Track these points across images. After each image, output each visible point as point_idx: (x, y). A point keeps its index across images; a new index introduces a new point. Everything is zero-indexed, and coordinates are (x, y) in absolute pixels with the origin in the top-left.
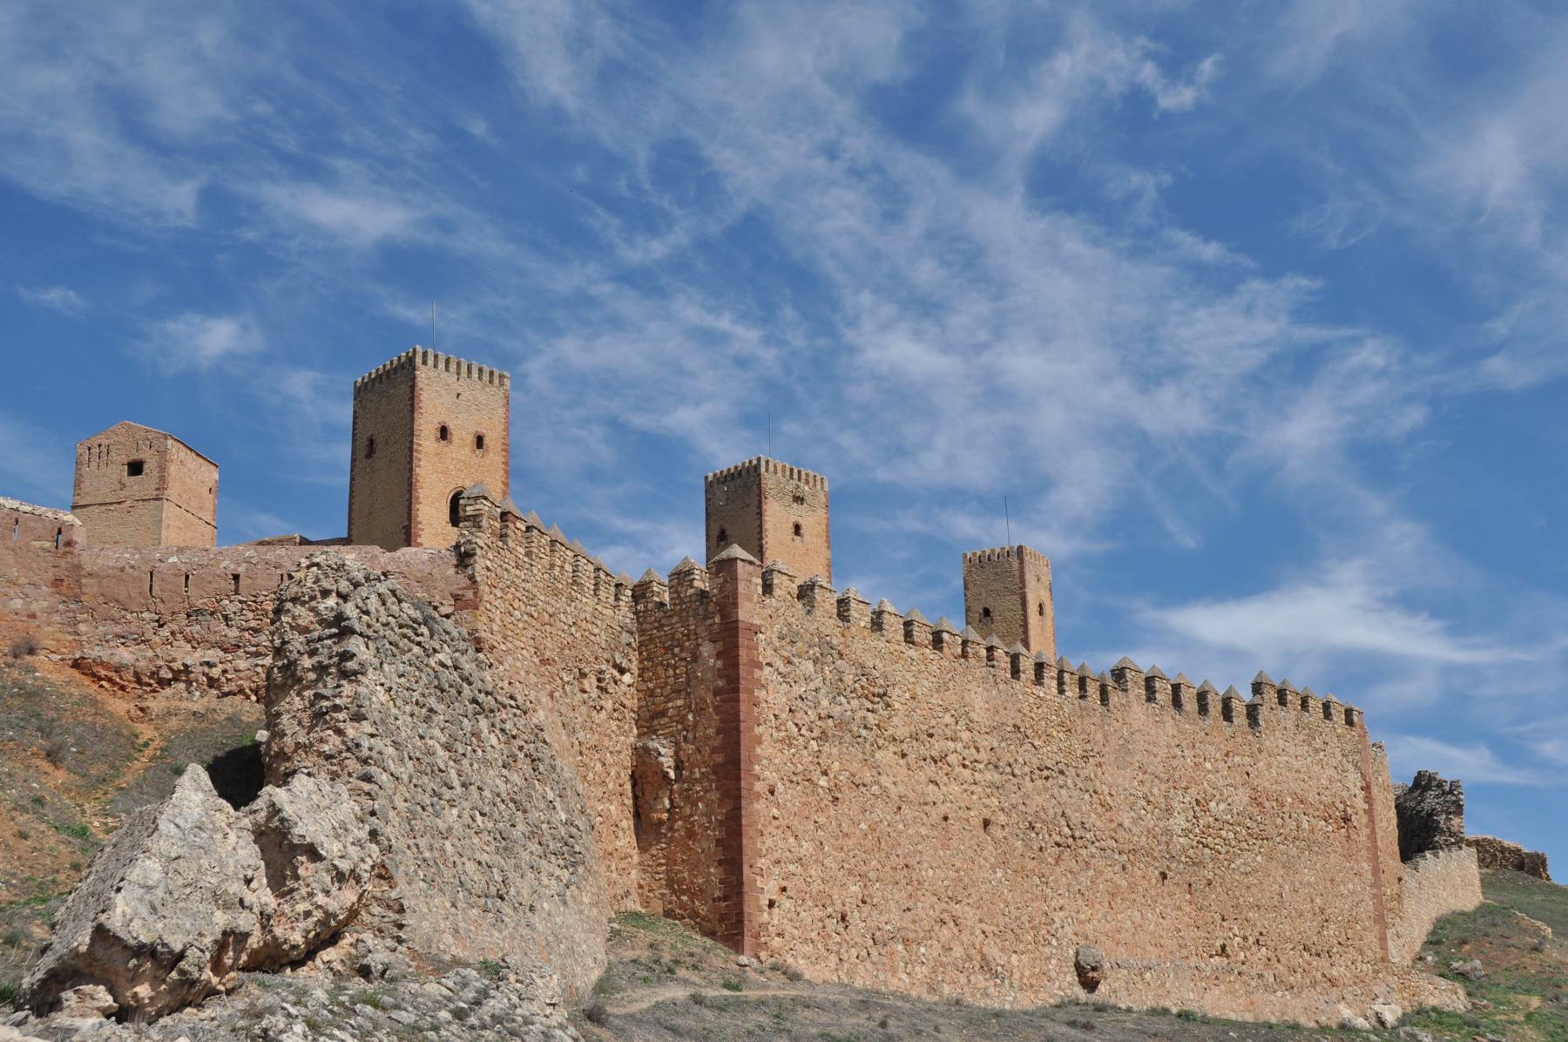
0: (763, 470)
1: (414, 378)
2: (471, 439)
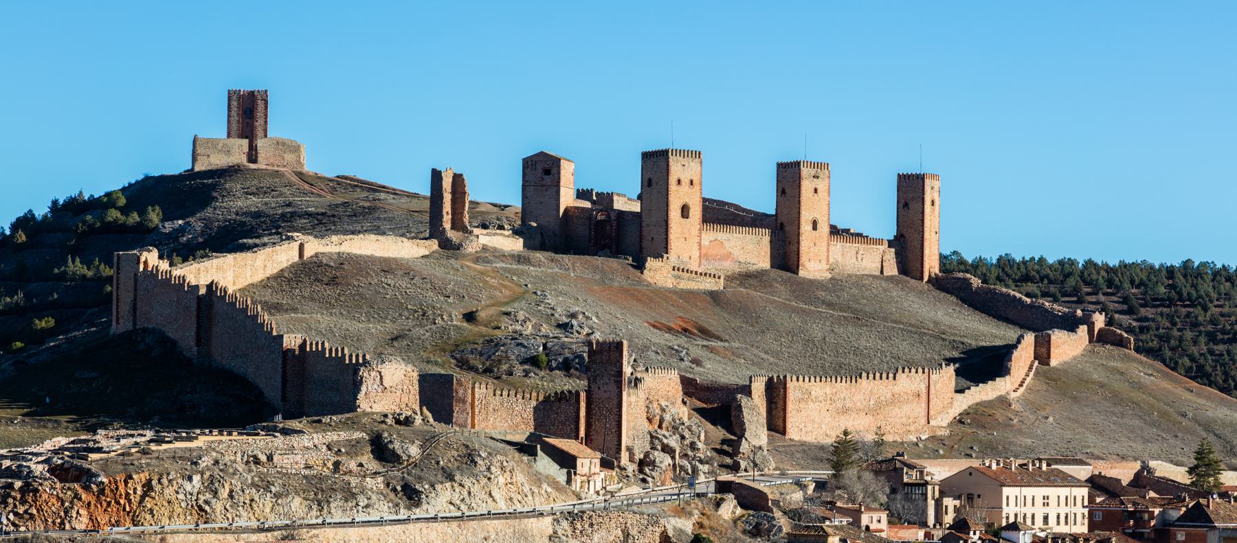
0: (802, 166)
1: (668, 162)
2: (688, 182)
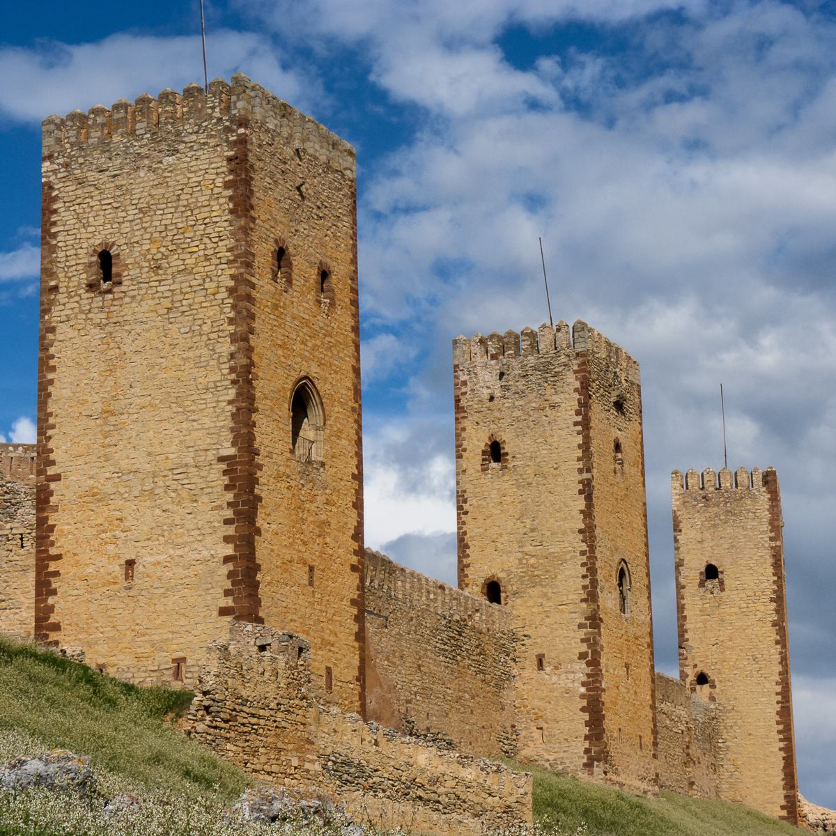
2: (313, 274)
